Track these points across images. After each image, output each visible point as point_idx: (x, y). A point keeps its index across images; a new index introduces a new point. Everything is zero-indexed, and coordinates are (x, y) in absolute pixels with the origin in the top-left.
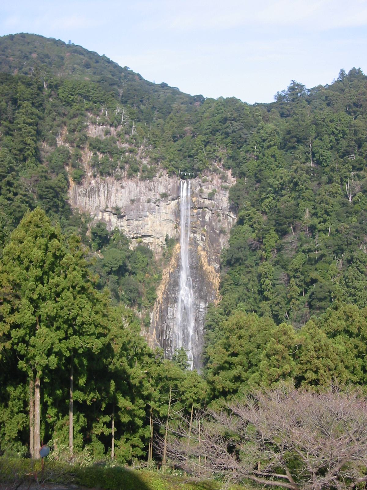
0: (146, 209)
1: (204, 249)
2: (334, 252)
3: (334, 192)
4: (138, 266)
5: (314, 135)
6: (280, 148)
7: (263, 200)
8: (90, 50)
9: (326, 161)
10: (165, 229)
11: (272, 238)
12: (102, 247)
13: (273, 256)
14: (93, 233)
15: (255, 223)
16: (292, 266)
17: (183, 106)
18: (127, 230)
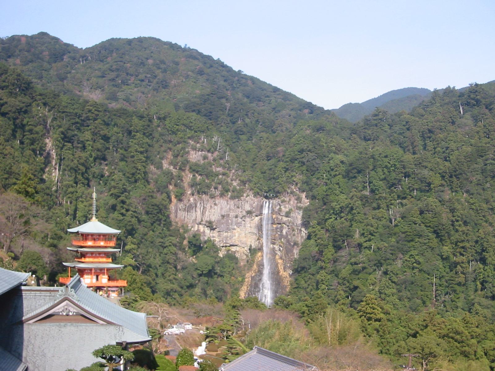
0: (234, 223)
1: (281, 258)
2: (375, 265)
3: (380, 216)
4: (225, 270)
5: (371, 167)
6: (344, 177)
7: (327, 219)
8: (205, 53)
9: (378, 190)
10: (249, 240)
11: (329, 252)
12: (196, 253)
13: (330, 266)
14: (189, 242)
15: (319, 239)
16: (341, 275)
17: (293, 113)
18: (217, 240)
